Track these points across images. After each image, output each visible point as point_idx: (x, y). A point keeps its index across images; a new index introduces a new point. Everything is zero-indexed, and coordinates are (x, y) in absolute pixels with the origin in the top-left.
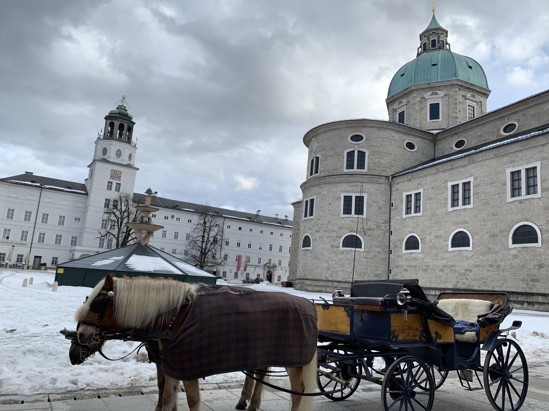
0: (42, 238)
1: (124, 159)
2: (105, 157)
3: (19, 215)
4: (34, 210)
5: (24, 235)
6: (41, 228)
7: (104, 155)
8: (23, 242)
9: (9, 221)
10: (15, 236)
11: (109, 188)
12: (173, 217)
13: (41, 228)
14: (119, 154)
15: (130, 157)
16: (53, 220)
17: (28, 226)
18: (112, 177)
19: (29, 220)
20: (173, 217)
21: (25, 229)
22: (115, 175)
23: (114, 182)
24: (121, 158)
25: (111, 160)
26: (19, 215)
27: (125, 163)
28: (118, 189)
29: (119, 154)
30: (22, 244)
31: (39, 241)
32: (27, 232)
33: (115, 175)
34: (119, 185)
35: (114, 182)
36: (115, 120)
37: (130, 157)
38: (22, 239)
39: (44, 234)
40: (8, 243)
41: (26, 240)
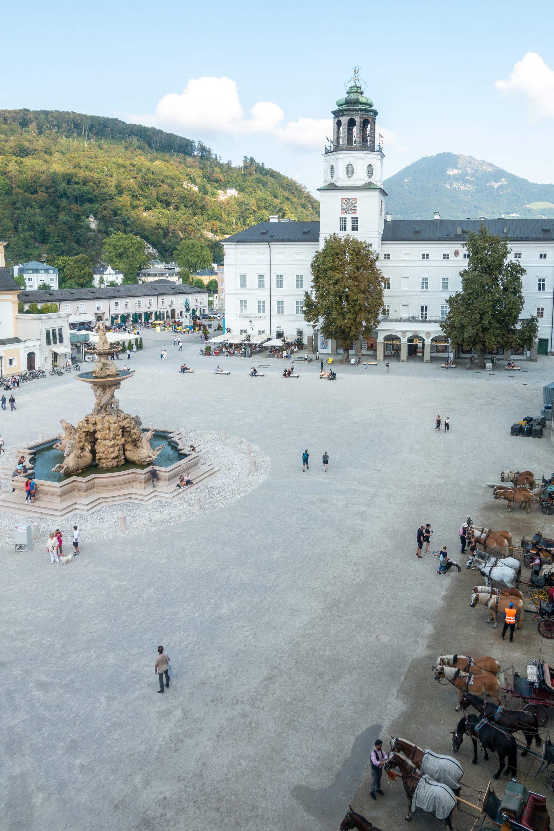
0: (280, 307)
1: (360, 177)
2: (334, 181)
3: (252, 281)
4: (265, 271)
5: (261, 304)
6: (278, 294)
7: (332, 177)
8: (262, 314)
9: (243, 291)
10: (252, 308)
11: (343, 227)
12: (457, 253)
13: (278, 294)
14: (350, 170)
15: (370, 170)
16: (290, 282)
17: (263, 294)
18: (344, 210)
19: (263, 286)
20: (457, 253)
21: (261, 298)
22: (349, 206)
23: (349, 217)
24: (354, 177)
25: (339, 184)
26: (252, 281)
27: (360, 184)
28: (355, 227)
29: (350, 170)
30: (261, 317)
31: (278, 312)
32: (263, 302)
33: (349, 206)
34: (355, 221)
35: (349, 217)
36: (342, 116)
37: (370, 170)
38: (259, 311)
39: (282, 302)
40: (246, 317)
41: (264, 312)
